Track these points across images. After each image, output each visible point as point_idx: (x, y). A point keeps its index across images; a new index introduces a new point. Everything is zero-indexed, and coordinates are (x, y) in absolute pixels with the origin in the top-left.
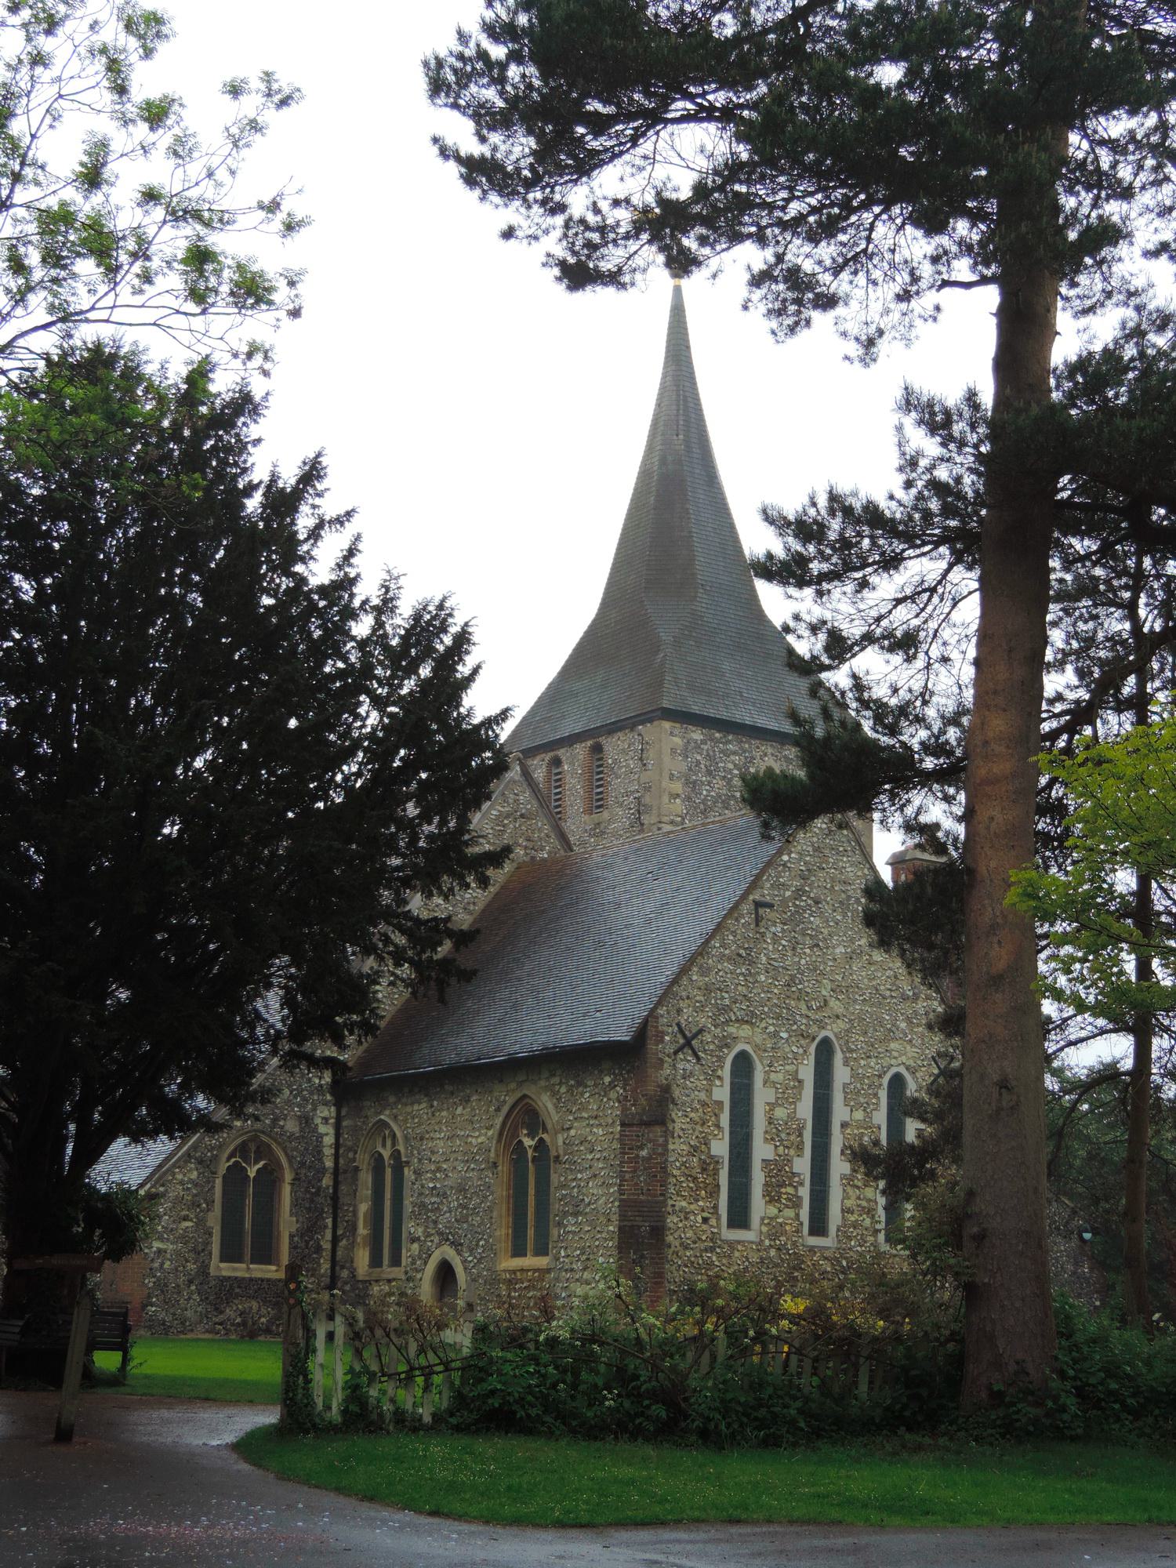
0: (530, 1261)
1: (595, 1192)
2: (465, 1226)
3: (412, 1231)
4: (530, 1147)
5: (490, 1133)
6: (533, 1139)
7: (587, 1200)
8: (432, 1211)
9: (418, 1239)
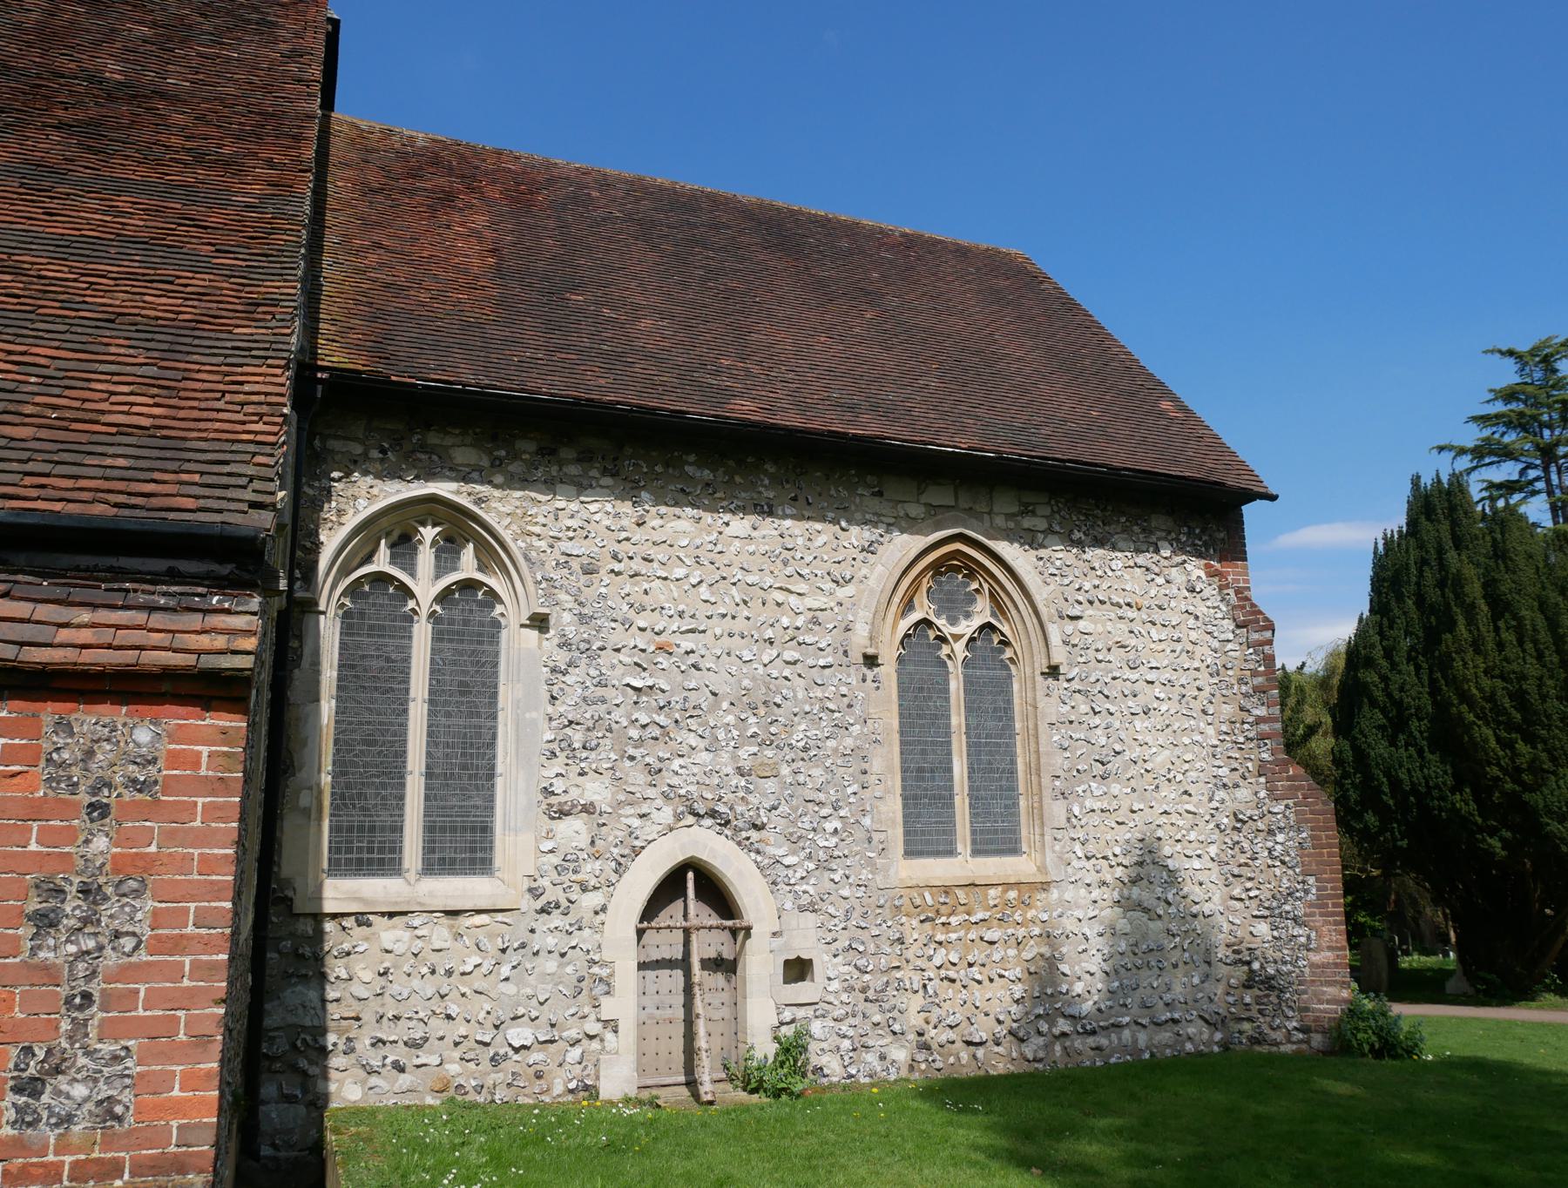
0: (962, 866)
1: (1149, 739)
2: (770, 785)
3: (559, 786)
4: (957, 637)
5: (843, 593)
6: (953, 621)
7: (1127, 755)
8: (640, 742)
9: (588, 809)
